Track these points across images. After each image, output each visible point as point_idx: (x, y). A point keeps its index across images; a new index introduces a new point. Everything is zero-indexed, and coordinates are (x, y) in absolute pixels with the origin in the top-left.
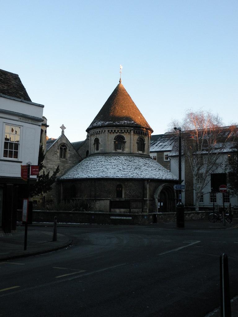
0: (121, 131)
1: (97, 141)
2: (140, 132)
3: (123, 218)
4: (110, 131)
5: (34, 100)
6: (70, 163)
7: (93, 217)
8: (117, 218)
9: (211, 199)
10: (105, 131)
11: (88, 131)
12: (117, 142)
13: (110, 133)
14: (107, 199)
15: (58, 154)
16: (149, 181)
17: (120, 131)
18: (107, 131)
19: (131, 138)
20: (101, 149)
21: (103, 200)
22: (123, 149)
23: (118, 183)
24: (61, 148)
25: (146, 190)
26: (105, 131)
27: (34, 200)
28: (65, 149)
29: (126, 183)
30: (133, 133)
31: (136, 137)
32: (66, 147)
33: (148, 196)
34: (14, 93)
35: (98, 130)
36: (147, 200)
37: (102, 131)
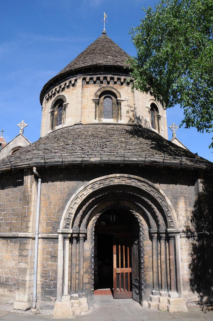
16: (35, 170)
33: (30, 224)
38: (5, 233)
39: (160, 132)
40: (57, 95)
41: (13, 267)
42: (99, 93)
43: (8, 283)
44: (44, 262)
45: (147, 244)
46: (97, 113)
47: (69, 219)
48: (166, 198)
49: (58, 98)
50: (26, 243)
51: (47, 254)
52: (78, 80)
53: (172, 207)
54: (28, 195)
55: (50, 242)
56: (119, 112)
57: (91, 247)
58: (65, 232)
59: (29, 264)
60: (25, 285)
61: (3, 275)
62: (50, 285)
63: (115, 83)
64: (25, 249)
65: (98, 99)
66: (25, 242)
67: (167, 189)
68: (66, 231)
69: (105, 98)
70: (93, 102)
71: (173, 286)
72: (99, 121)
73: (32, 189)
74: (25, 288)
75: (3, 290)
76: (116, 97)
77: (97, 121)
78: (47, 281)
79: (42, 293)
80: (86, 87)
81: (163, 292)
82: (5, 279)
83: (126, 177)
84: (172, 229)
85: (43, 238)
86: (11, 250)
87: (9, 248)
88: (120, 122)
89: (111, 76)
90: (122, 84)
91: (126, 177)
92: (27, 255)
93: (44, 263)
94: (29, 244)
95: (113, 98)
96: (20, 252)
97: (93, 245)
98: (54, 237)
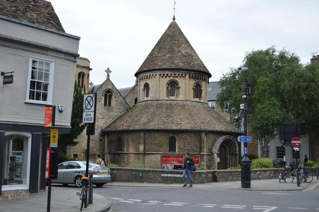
0: (175, 74)
1: (147, 86)
3: (176, 176)
4: (162, 75)
5: (68, 30)
6: (116, 112)
7: (141, 174)
8: (169, 175)
9: (278, 154)
10: (156, 75)
11: (136, 75)
12: (170, 88)
13: (162, 77)
14: (158, 154)
15: (103, 102)
17: (173, 75)
18: (158, 75)
19: (186, 83)
20: (152, 95)
21: (154, 154)
22: (177, 96)
23: (171, 135)
24: (106, 96)
26: (156, 75)
28: (110, 97)
29: (180, 135)
32: (112, 93)
34: (44, 22)
35: (148, 74)
37: (153, 75)
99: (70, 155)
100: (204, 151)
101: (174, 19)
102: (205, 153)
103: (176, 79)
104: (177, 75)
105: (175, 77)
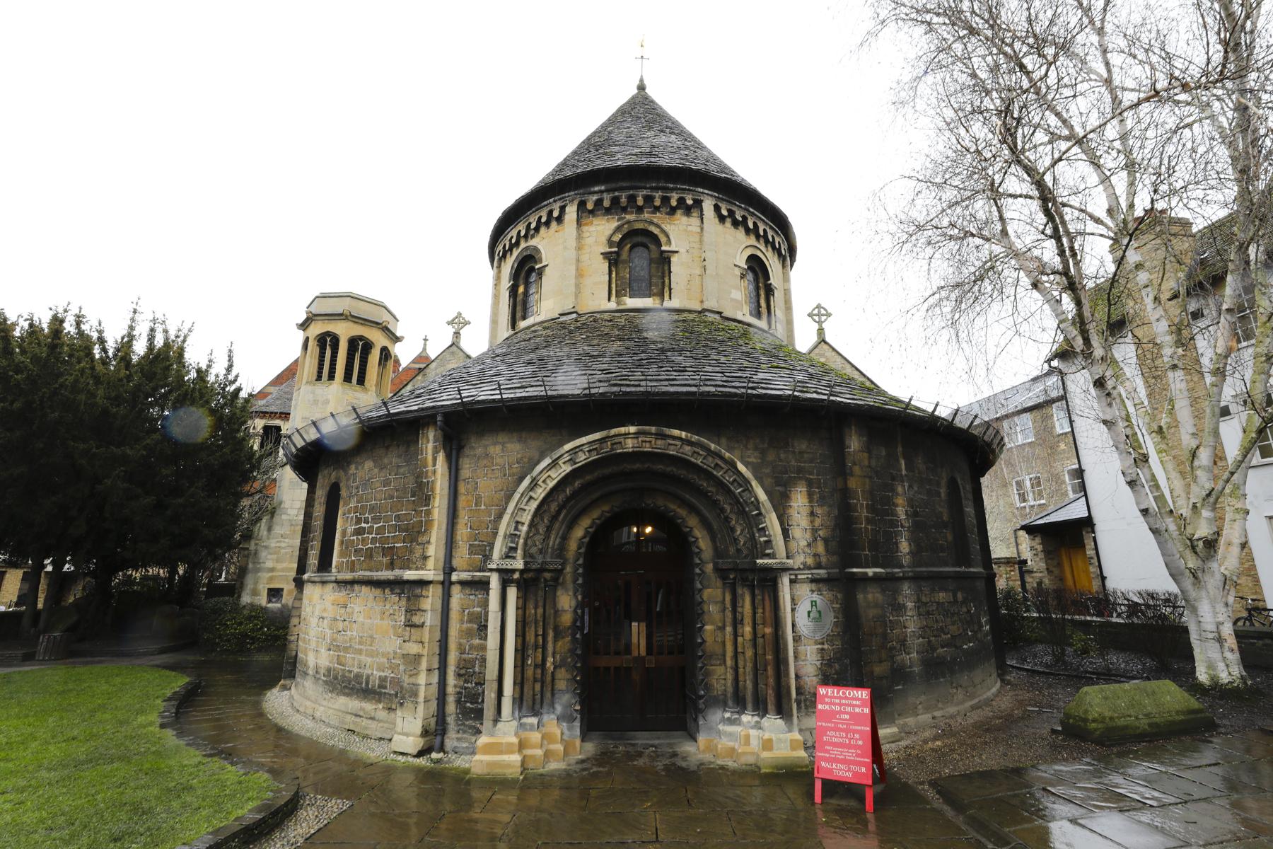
2: (624, 200)
25: (427, 500)
27: (272, 586)
30: (575, 216)
31: (602, 230)
36: (423, 583)
38: (379, 573)
39: (773, 327)
40: (523, 245)
41: (395, 653)
42: (617, 237)
43: (383, 691)
44: (462, 641)
45: (713, 597)
46: (614, 286)
47: (516, 535)
48: (754, 483)
49: (525, 254)
50: (422, 596)
51: (470, 621)
52: (567, 209)
53: (768, 505)
54: (428, 482)
55: (477, 593)
56: (667, 281)
57: (574, 603)
58: (504, 567)
59: (426, 645)
60: (415, 694)
61: (375, 672)
62: (475, 695)
63: (657, 209)
64: (419, 610)
65: (615, 252)
66: (418, 591)
67: (759, 461)
68: (509, 564)
69: (631, 248)
70: (604, 258)
71: (771, 706)
72: (618, 303)
73: (437, 467)
74: (417, 703)
75: (374, 707)
76: (659, 244)
77: (613, 305)
78: (469, 685)
79: (457, 714)
80: (586, 224)
81: (746, 718)
82: (377, 681)
83: (652, 434)
84: (770, 561)
85: (463, 583)
86: (391, 611)
87: (387, 607)
88: (667, 304)
89: (645, 192)
90: (673, 211)
91: (652, 434)
92: (423, 623)
93: (464, 641)
94: (428, 597)
95: (652, 247)
96: (408, 617)
97: (580, 597)
98: (483, 579)
99: (255, 593)
100: (425, 558)
101: (642, 87)
102: (430, 572)
103: (532, 242)
104: (533, 226)
105: (533, 237)
